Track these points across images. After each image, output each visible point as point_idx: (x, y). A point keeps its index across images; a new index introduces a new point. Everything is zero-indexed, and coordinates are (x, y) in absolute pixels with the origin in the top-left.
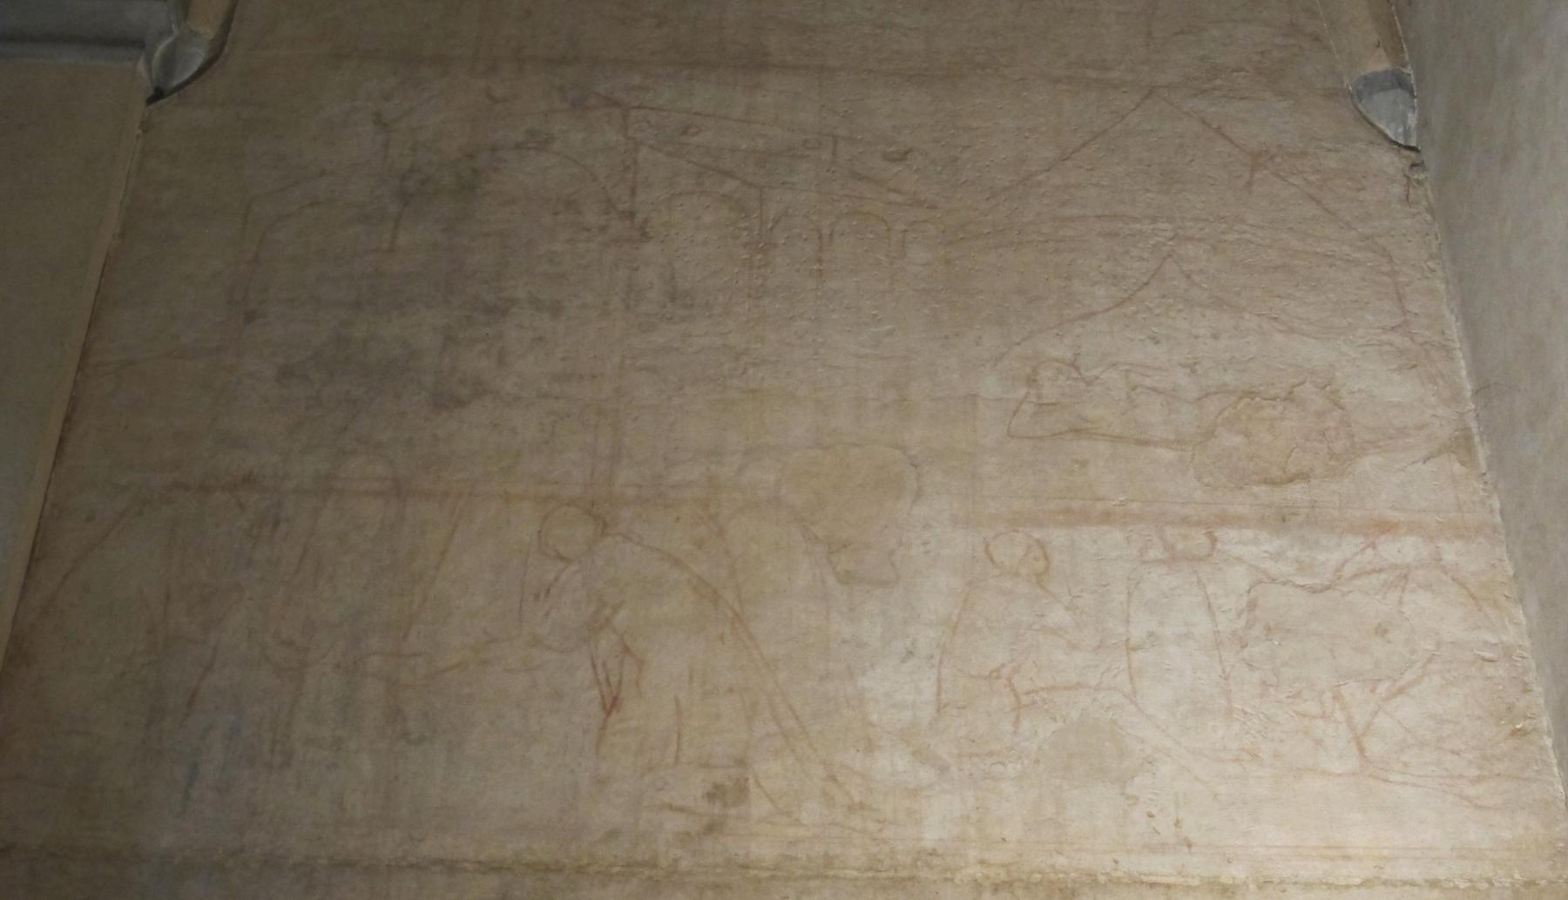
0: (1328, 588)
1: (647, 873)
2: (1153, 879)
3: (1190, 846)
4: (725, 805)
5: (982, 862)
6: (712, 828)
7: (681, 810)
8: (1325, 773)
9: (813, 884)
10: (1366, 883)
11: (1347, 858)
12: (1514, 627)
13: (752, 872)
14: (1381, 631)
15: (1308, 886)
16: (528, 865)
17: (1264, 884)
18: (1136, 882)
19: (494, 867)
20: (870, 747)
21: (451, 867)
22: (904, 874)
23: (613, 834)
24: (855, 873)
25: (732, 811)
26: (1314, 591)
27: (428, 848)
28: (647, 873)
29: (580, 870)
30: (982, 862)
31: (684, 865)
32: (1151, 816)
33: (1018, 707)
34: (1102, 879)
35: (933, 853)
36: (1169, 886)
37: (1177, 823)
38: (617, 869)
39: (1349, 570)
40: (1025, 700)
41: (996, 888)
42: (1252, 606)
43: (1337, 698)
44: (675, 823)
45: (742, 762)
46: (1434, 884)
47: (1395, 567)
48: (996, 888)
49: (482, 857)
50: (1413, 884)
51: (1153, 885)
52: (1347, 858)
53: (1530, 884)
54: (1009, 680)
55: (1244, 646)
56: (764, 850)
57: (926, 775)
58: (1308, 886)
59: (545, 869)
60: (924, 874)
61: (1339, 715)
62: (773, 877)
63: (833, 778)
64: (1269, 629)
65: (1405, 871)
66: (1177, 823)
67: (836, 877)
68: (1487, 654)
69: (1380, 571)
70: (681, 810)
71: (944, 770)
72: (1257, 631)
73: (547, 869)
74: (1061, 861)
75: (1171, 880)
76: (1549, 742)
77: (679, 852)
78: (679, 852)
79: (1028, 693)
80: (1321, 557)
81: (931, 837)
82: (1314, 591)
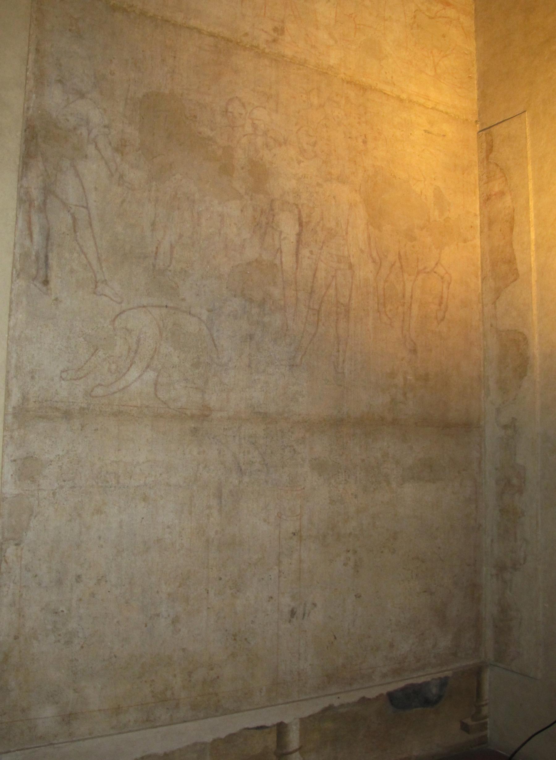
0: (433, 18)
1: (256, 50)
2: (385, 92)
3: (394, 85)
4: (278, 34)
5: (345, 74)
6: (275, 41)
7: (266, 32)
8: (426, 74)
9: (301, 67)
10: (432, 108)
11: (429, 100)
12: (472, 46)
13: (285, 59)
14: (444, 36)
15: (420, 105)
16: (222, 37)
17: (410, 101)
18: (381, 91)
19: (212, 35)
20: (317, 28)
21: (200, 31)
22: (325, 71)
23: (246, 34)
24: (312, 67)
25: (280, 37)
26: (430, 18)
27: (192, 23)
28: (256, 50)
29: (237, 43)
30: (345, 74)
31: (267, 50)
32: (386, 73)
33: (356, 28)
34: (373, 88)
35: (332, 67)
36: (388, 95)
37: (392, 77)
38: (248, 46)
39: (438, 15)
40: (358, 27)
41: (348, 82)
42: (415, 17)
43: (431, 52)
44: (264, 36)
45: (283, 22)
46: (447, 113)
47: (448, 17)
48: (348, 82)
49: (209, 30)
50: (442, 112)
51: (385, 93)
52: (429, 100)
53: (467, 120)
54: (354, 19)
55: (412, 29)
56: (289, 52)
57: (332, 42)
58: (420, 105)
59: (228, 40)
60: (330, 73)
61: (431, 58)
62: (291, 62)
63: (307, 35)
64: (418, 26)
65: (441, 108)
66: (392, 77)
67: (307, 67)
68: (466, 52)
69: (446, 17)
70: (266, 32)
71: (336, 42)
72: (415, 25)
73: (228, 40)
74: (364, 79)
75: (389, 93)
76: (476, 82)
77: (265, 46)
78: (265, 46)
79: (359, 25)
80: (433, 8)
81: (332, 62)
82: (430, 18)
